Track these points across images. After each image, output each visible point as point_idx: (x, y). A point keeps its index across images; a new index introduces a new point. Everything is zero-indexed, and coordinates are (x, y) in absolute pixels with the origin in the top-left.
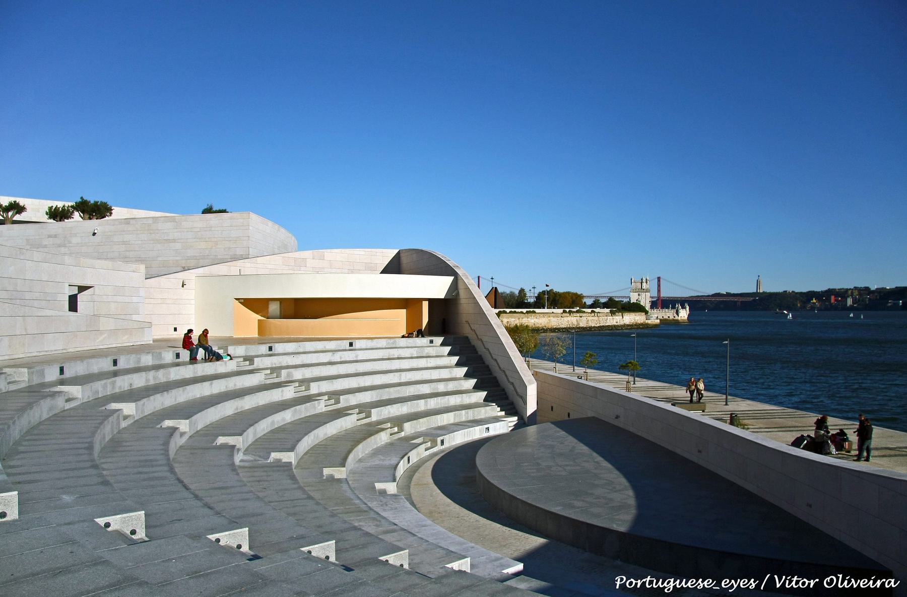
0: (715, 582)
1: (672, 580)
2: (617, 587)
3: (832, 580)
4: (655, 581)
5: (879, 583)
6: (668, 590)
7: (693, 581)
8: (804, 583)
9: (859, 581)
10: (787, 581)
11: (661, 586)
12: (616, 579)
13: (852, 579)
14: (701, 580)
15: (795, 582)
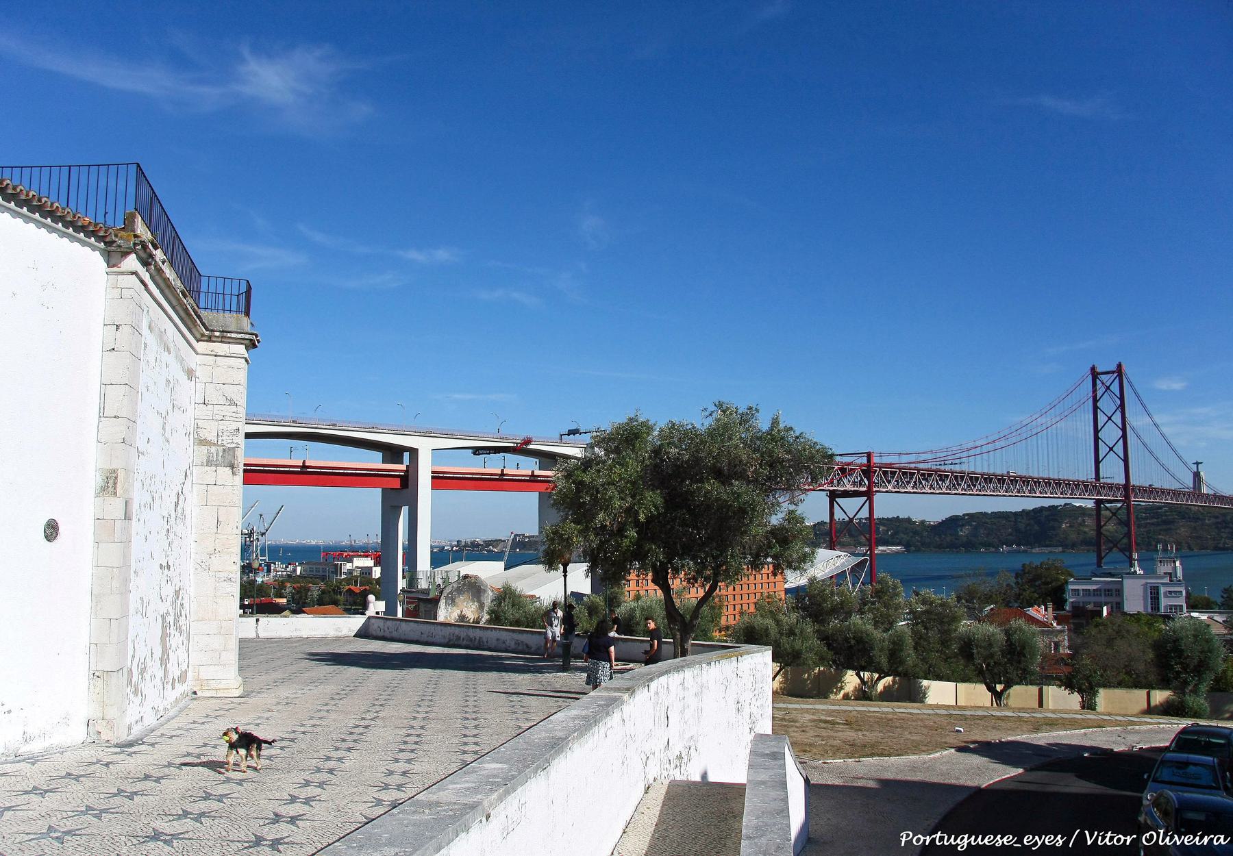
0: (1016, 838)
1: (966, 836)
2: (903, 845)
3: (1152, 836)
4: (946, 837)
5: (1206, 840)
6: (962, 848)
7: (990, 838)
8: (1119, 840)
9: (1183, 837)
10: (1100, 838)
11: (953, 843)
12: (901, 835)
13: (1175, 836)
14: (999, 836)
15: (1109, 839)
